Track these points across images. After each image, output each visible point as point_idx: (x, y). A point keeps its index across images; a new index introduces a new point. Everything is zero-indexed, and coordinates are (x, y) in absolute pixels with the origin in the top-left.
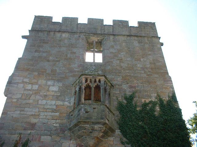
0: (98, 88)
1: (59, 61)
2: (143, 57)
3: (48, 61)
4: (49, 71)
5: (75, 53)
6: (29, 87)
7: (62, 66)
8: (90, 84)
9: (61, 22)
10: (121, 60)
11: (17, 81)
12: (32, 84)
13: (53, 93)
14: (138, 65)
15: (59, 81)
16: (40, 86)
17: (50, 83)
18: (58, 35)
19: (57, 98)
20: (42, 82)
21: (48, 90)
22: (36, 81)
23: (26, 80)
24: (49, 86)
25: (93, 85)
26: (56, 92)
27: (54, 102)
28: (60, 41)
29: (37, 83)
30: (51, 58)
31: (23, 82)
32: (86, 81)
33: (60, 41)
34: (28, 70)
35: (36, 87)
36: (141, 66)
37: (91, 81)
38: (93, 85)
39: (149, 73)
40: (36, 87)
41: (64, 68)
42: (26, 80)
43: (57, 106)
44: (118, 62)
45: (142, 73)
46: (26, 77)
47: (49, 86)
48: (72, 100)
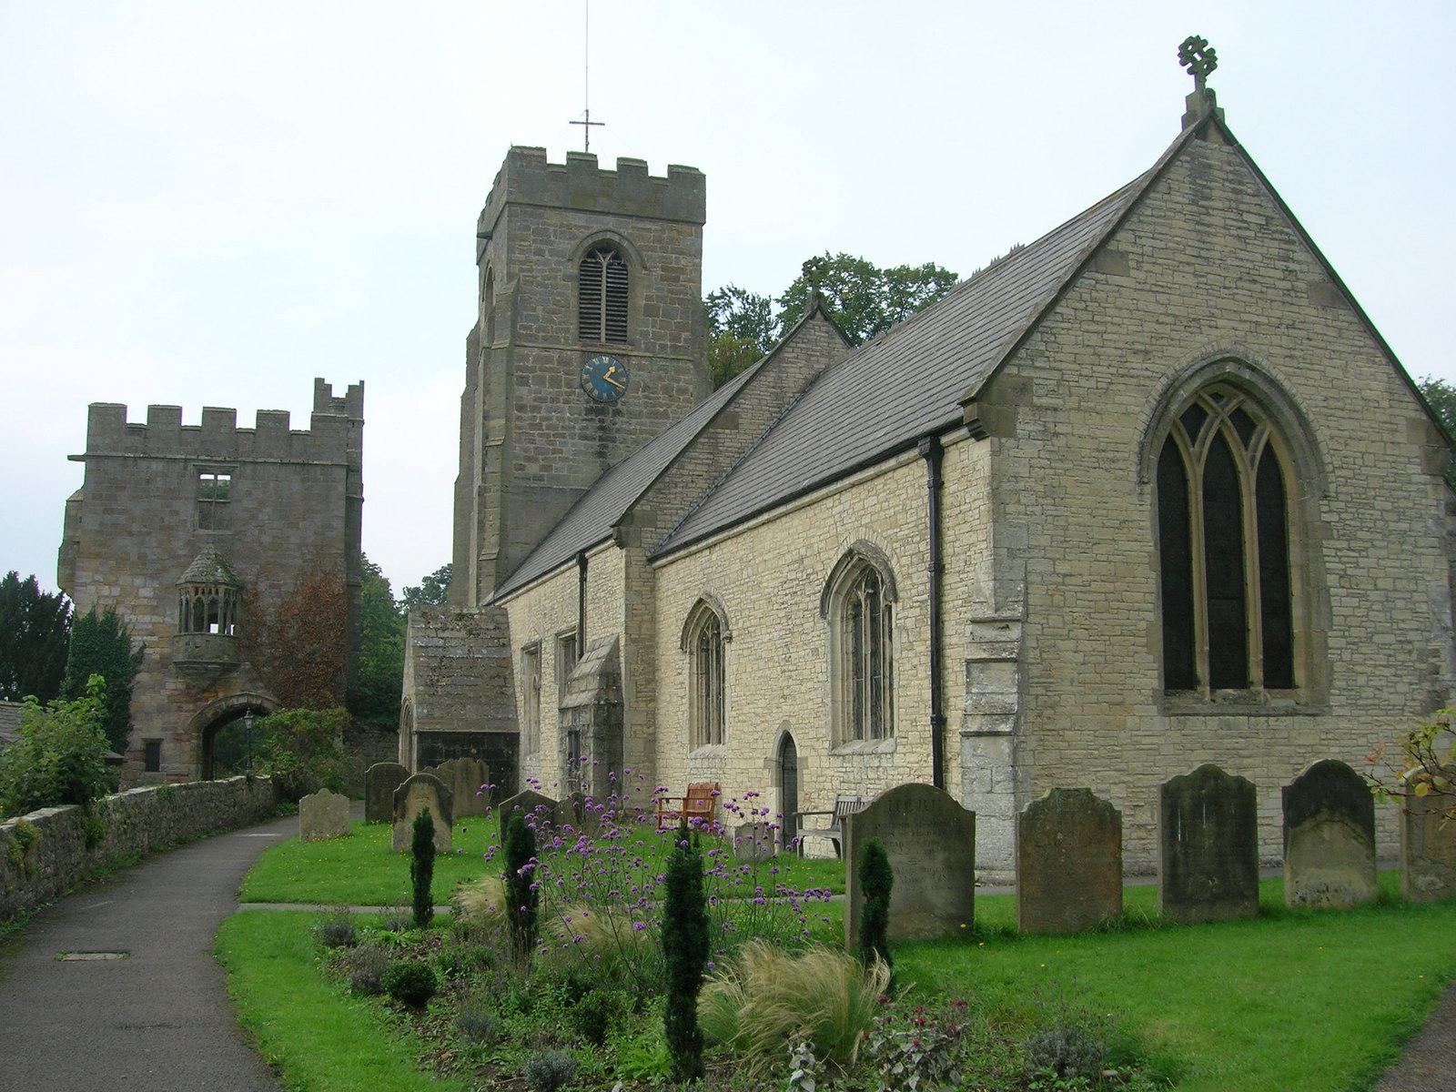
0: (213, 603)
1: (149, 534)
2: (304, 520)
3: (131, 534)
4: (134, 557)
5: (177, 513)
6: (105, 591)
7: (155, 544)
8: (203, 598)
9: (145, 423)
10: (261, 527)
11: (84, 580)
12: (110, 585)
13: (145, 601)
14: (292, 539)
15: (153, 577)
16: (123, 589)
17: (138, 581)
18: (143, 465)
19: (154, 610)
20: (125, 579)
21: (137, 597)
22: (115, 579)
23: (98, 577)
24: (138, 588)
25: (206, 600)
26: (149, 598)
27: (147, 619)
28: (148, 482)
29: (115, 583)
30: (135, 528)
31: (95, 582)
32: (196, 593)
33: (148, 482)
34: (98, 555)
35: (116, 591)
36: (298, 541)
37: (203, 593)
38: (206, 600)
39: (308, 557)
40: (116, 591)
41: (159, 550)
42: (98, 577)
43: (154, 624)
44: (256, 533)
45: (296, 557)
46: (96, 572)
47: (138, 588)
48: (177, 613)
